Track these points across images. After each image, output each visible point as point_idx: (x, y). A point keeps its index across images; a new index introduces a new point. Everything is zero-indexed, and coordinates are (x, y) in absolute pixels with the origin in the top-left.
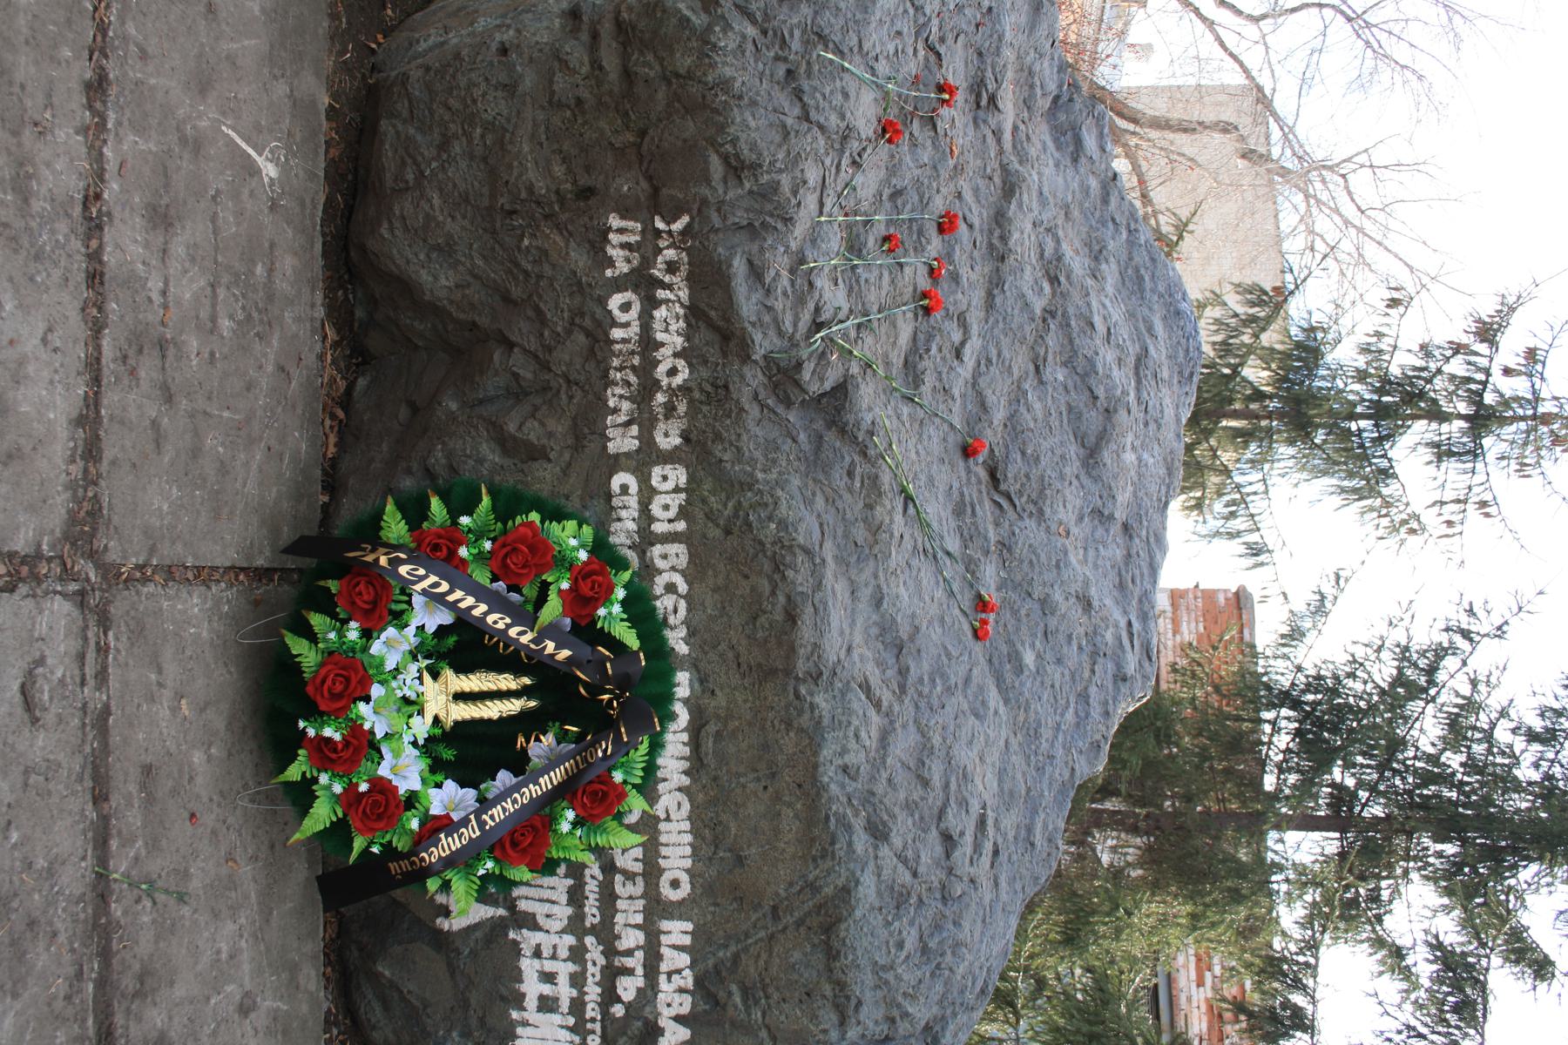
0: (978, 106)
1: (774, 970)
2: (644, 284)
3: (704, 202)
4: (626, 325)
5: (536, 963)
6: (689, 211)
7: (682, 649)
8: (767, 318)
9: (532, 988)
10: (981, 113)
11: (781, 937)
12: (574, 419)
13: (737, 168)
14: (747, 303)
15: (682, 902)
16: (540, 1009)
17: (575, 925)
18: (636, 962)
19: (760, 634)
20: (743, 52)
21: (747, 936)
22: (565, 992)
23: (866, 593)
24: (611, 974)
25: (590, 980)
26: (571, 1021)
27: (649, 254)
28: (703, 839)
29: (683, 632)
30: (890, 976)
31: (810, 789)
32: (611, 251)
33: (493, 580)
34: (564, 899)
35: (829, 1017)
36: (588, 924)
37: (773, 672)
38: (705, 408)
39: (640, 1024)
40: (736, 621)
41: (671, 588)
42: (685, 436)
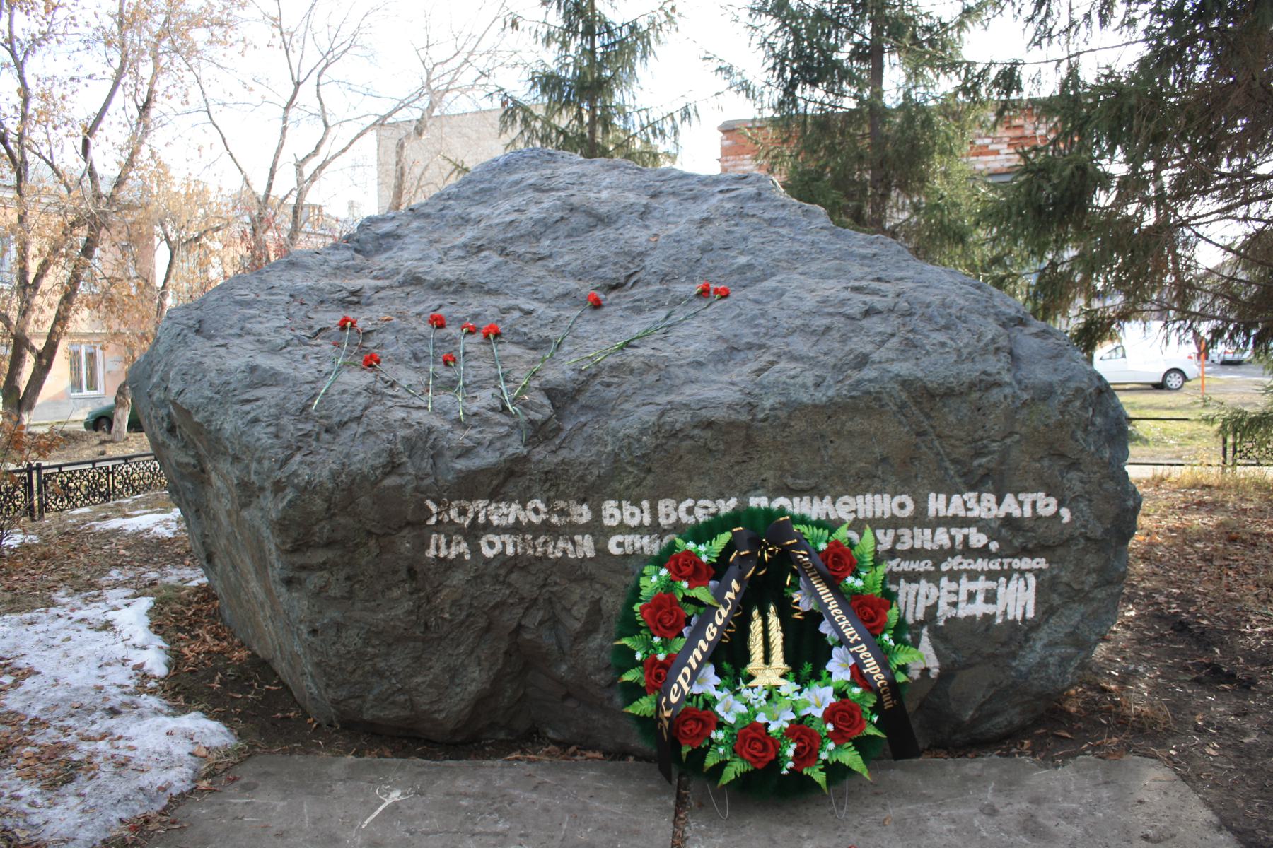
0: (358, 303)
1: (962, 434)
2: (474, 532)
3: (416, 489)
4: (504, 544)
5: (961, 605)
6: (423, 500)
7: (733, 502)
8: (498, 444)
9: (979, 608)
10: (363, 301)
11: (938, 429)
12: (571, 581)
13: (393, 467)
14: (487, 458)
15: (915, 502)
16: (994, 602)
17: (933, 577)
18: (959, 534)
19: (722, 447)
20: (313, 463)
21: (938, 454)
22: (982, 585)
23: (693, 373)
24: (968, 551)
25: (973, 567)
26: (1003, 580)
27: (453, 528)
28: (869, 486)
29: (721, 502)
30: (965, 352)
31: (831, 409)
33: (681, 635)
34: (914, 586)
35: (996, 394)
36: (933, 569)
37: (748, 438)
38: (562, 488)
39: (1003, 531)
40: (712, 464)
41: (690, 511)
42: (582, 501)
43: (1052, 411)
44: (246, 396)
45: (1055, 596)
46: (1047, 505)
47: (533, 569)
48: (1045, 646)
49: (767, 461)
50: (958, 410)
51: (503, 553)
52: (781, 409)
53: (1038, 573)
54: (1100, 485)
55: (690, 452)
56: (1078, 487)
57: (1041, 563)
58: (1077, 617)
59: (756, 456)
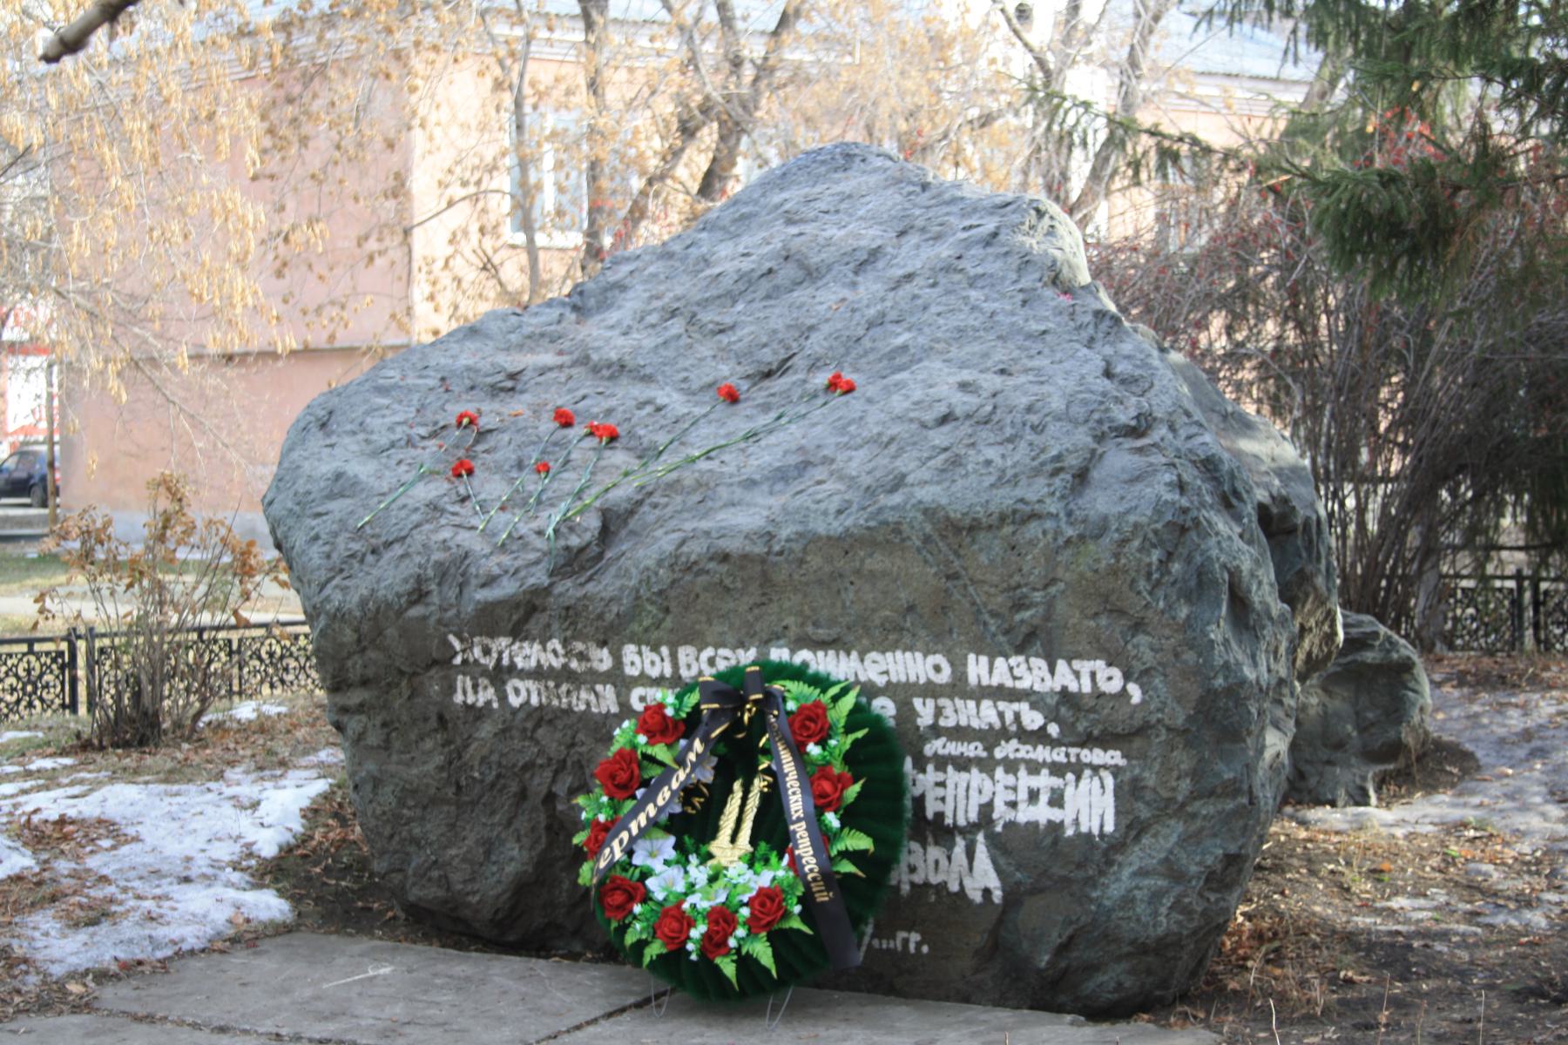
0: (512, 389)
1: (995, 579)
2: (500, 675)
3: (439, 621)
4: (528, 691)
5: (1022, 806)
6: (445, 635)
7: (752, 654)
8: (523, 573)
9: (1042, 813)
10: (519, 387)
11: (971, 571)
13: (419, 595)
14: (507, 588)
15: (952, 664)
18: (1009, 709)
19: (739, 585)
20: (347, 588)
21: (974, 603)
22: (1044, 781)
23: (738, 493)
24: (1025, 736)
25: (1032, 756)
26: (1070, 777)
27: (479, 670)
29: (740, 652)
30: (1010, 473)
31: (845, 544)
32: (480, 703)
33: (633, 797)
34: (964, 776)
35: (1033, 529)
36: (984, 754)
37: (764, 573)
38: (580, 626)
40: (731, 605)
41: (712, 662)
42: (603, 644)
43: (1100, 553)
44: (320, 509)
45: (1140, 805)
46: (1110, 678)
47: (560, 724)
48: (1135, 874)
49: (787, 604)
50: (990, 548)
51: (527, 702)
52: (797, 541)
53: (1116, 771)
54: (1177, 655)
55: (706, 589)
56: (1149, 657)
57: (1114, 757)
58: (1174, 839)
59: (775, 598)
